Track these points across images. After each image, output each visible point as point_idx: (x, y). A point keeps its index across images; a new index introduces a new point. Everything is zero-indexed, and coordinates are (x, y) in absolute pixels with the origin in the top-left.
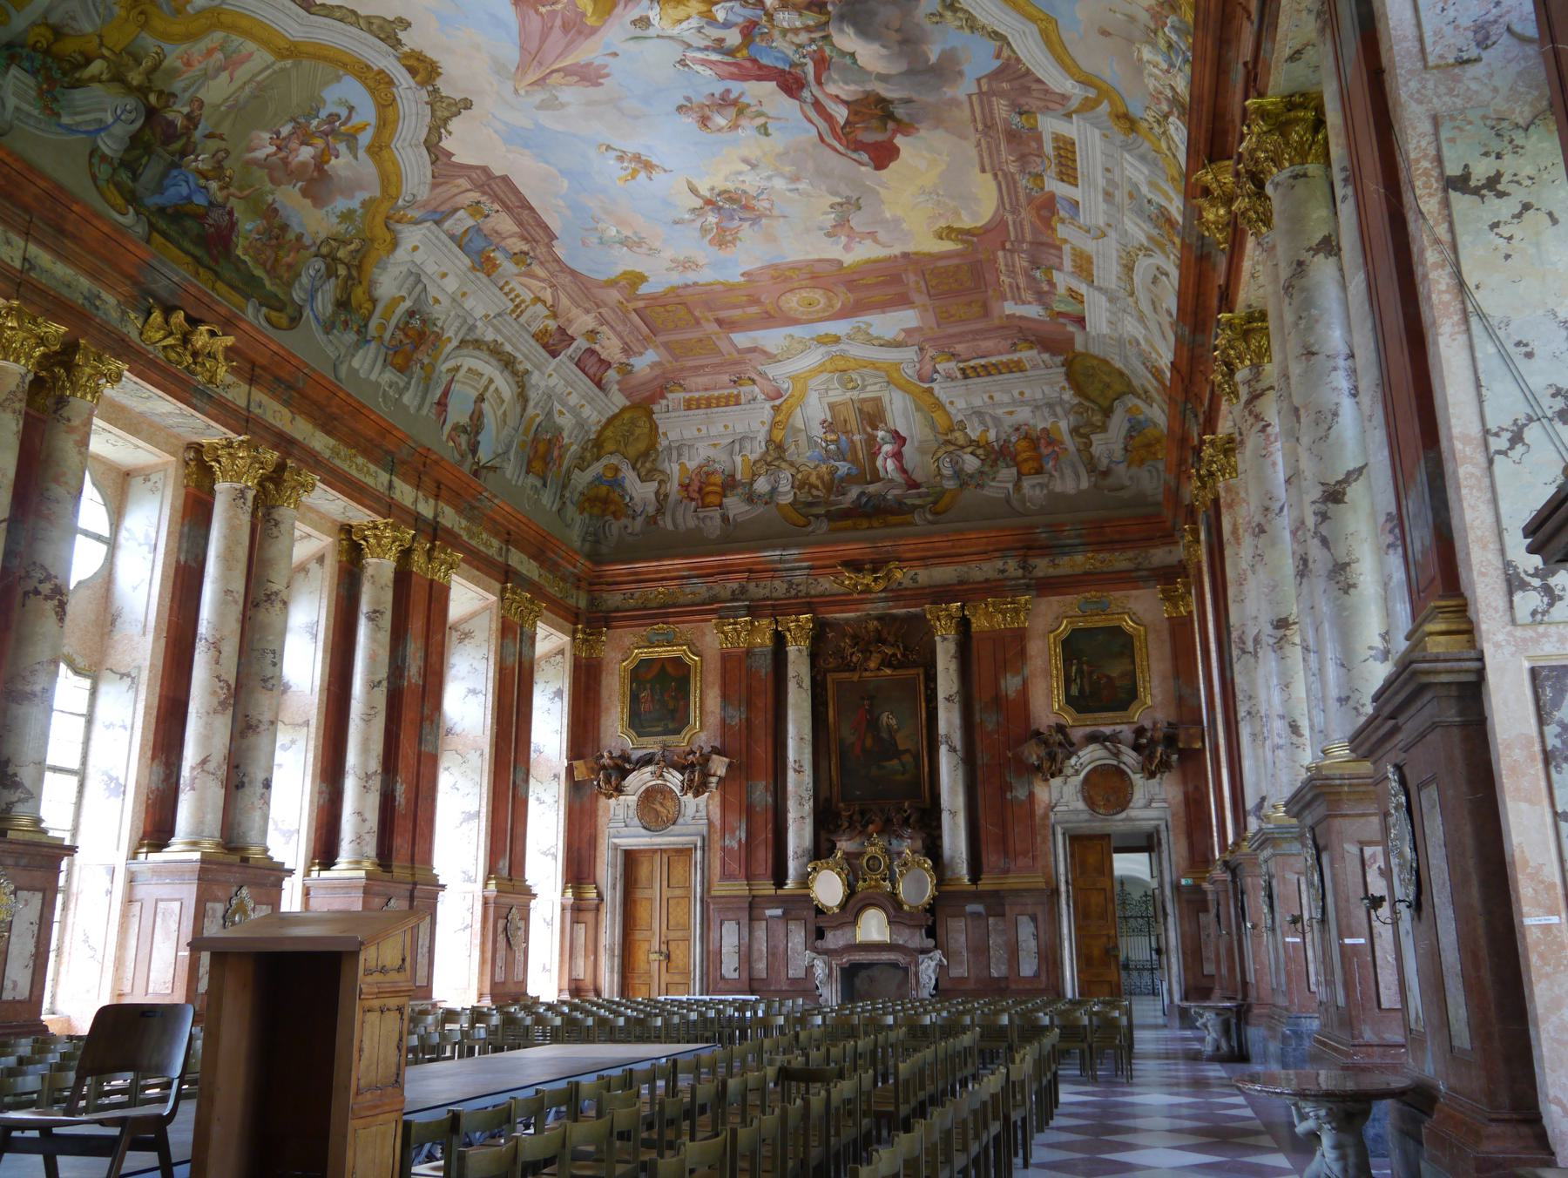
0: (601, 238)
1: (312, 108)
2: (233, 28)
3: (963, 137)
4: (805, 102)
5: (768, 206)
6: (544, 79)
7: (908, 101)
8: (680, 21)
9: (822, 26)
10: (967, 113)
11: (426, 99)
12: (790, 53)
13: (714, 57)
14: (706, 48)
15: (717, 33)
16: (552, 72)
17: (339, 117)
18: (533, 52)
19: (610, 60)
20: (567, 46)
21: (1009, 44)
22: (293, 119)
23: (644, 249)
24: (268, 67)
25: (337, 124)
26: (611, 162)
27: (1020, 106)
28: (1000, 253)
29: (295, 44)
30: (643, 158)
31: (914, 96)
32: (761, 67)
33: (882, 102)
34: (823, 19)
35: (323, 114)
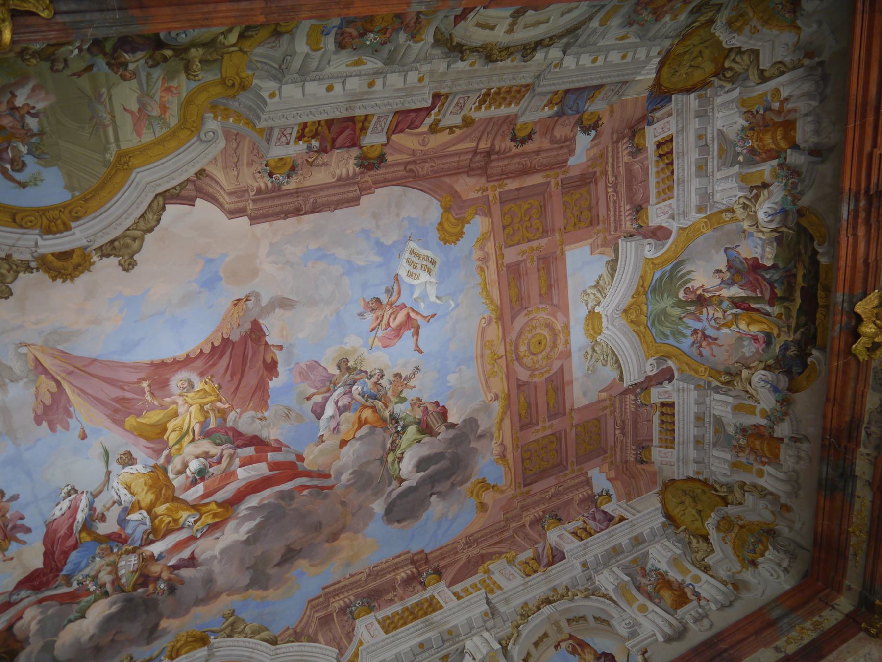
1: (43, 153)
2: (174, 134)
6: (46, 372)
8: (128, 488)
9: (120, 589)
11: (16, 257)
12: (86, 571)
13: (80, 517)
14: (92, 508)
15: (113, 514)
16: (59, 384)
17: (19, 171)
18: (86, 369)
19: (78, 432)
20: (100, 401)
22: (41, 133)
24: (117, 139)
25: (8, 166)
29: (129, 170)
32: (66, 554)
34: (128, 588)
35: (29, 160)
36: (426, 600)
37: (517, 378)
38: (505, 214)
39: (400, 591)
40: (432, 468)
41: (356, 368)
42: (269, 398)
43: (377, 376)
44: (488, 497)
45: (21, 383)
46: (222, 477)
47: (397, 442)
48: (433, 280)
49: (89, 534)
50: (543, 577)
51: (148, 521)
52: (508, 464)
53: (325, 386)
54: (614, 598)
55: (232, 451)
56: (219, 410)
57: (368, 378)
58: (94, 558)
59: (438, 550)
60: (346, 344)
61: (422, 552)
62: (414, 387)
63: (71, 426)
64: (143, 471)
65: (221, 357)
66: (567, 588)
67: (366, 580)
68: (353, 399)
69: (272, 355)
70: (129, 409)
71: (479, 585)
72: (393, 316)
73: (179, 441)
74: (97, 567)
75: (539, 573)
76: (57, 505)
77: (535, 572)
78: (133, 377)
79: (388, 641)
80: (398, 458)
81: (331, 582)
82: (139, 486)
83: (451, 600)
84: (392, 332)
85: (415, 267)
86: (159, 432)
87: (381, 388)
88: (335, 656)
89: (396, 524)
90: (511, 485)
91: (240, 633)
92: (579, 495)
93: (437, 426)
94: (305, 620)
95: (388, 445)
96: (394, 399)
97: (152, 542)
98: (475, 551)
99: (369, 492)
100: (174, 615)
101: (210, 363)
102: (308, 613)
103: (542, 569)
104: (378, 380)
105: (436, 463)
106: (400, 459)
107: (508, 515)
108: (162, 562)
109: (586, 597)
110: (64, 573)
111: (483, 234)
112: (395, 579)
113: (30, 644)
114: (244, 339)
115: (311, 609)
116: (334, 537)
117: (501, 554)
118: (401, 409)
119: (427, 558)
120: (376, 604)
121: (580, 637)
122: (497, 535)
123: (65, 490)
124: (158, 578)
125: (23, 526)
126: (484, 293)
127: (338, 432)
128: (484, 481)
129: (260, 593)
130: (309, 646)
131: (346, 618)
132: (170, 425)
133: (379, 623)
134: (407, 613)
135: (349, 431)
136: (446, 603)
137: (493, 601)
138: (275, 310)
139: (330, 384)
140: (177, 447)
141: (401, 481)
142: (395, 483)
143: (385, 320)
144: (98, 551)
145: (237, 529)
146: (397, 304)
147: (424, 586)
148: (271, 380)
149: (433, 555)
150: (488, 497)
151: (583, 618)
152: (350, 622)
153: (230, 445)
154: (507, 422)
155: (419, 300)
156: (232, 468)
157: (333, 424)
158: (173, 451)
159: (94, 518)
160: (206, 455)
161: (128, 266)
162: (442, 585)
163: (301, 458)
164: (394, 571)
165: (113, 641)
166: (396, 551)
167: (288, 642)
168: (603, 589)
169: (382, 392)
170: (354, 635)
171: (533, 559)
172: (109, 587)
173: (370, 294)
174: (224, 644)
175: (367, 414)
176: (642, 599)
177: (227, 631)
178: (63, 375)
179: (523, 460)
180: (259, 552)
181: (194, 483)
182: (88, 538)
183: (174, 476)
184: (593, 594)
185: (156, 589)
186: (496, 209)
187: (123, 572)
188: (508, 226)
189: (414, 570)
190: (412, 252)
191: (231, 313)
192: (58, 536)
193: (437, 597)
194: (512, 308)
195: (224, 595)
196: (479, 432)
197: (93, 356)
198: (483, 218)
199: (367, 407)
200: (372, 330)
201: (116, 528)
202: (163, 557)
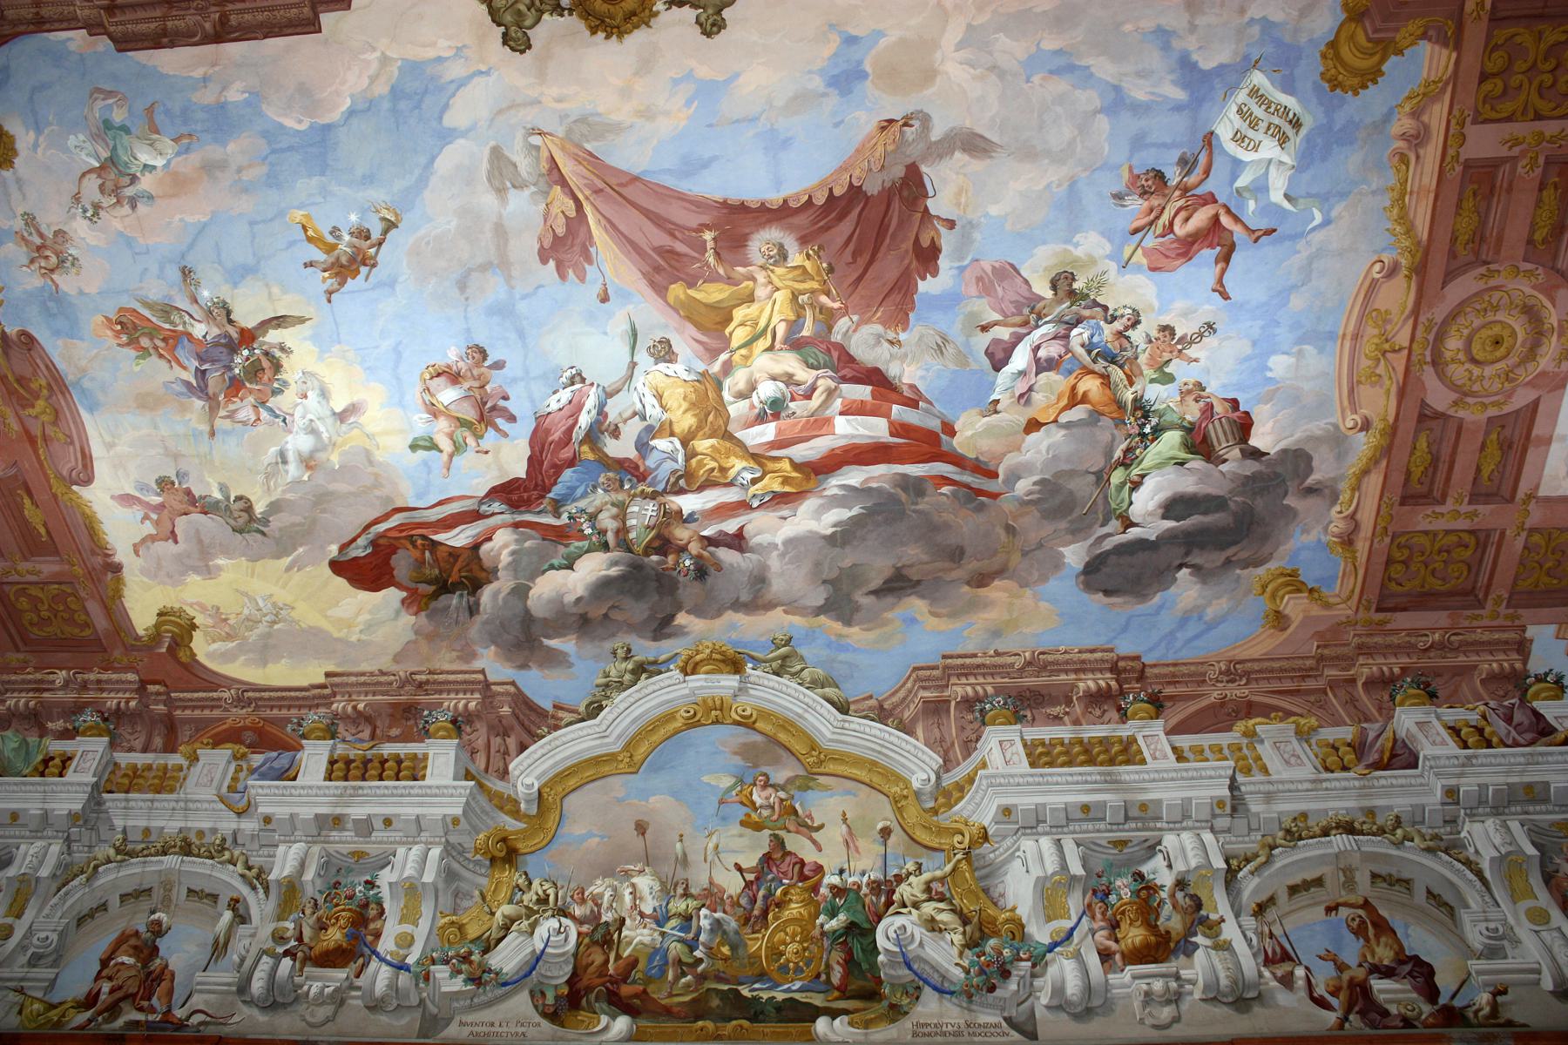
0: (125, 129)
3: (397, 658)
4: (481, 502)
5: (241, 415)
6: (563, 182)
7: (473, 610)
8: (659, 397)
9: (625, 544)
10: (447, 667)
12: (582, 504)
13: (584, 420)
15: (632, 430)
19: (598, 288)
21: (583, 720)
23: (91, 185)
26: (353, 218)
27: (470, 722)
28: (131, 677)
30: (364, 270)
31: (478, 619)
32: (558, 469)
33: (475, 586)
36: (1120, 740)
37: (1423, 401)
38: (1496, 48)
39: (1078, 709)
40: (1194, 520)
41: (1087, 295)
42: (913, 309)
43: (1125, 319)
44: (1295, 606)
45: (527, 192)
46: (808, 422)
47: (1138, 451)
48: (1286, 159)
49: (592, 450)
50: (1357, 783)
51: (680, 457)
52: (1355, 558)
53: (1020, 314)
54: (1487, 874)
55: (833, 384)
56: (822, 309)
57: (1106, 321)
58: (595, 487)
59: (1168, 665)
60: (1077, 245)
61: (1138, 658)
62: (1196, 360)
63: (589, 277)
64: (685, 376)
65: (842, 217)
66: (1398, 822)
67: (1022, 668)
68: (1068, 351)
69: (932, 233)
70: (678, 270)
71: (1226, 752)
72: (1183, 214)
73: (748, 344)
74: (598, 503)
75: (1351, 774)
76: (555, 393)
77: (1345, 768)
78: (693, 220)
79: (1030, 779)
80: (1131, 482)
81: (959, 651)
82: (677, 398)
83: (1165, 757)
84: (1175, 245)
85: (1253, 125)
86: (718, 319)
87: (1128, 345)
88: (935, 768)
89: (1101, 594)
90: (1349, 598)
91: (793, 675)
92: (1490, 664)
93: (1224, 445)
94: (901, 694)
95: (1118, 454)
96: (1149, 373)
97: (681, 491)
98: (1237, 691)
99: (1063, 525)
100: (698, 611)
101: (821, 224)
102: (909, 685)
103: (1360, 769)
104: (1127, 329)
105: (1205, 513)
106: (1136, 485)
107: (1326, 652)
108: (693, 526)
109: (1429, 850)
110: (551, 495)
111: (1427, 84)
112: (1074, 686)
113: (498, 579)
114: (889, 194)
115: (915, 681)
116: (981, 580)
117: (1289, 714)
118: (1158, 394)
119: (1143, 671)
120: (1029, 714)
121: (1383, 912)
122: (1292, 678)
123: (568, 374)
124: (683, 549)
125: (505, 410)
126: (1395, 211)
127: (1028, 402)
128: (1293, 574)
129: (837, 626)
130: (899, 737)
131: (970, 717)
132: (739, 314)
133: (1025, 745)
134: (1077, 749)
135: (1048, 407)
136: (1155, 758)
137: (1243, 788)
138: (953, 154)
139: (1029, 312)
140: (743, 351)
141: (1128, 524)
142: (1115, 524)
143: (1165, 218)
144: (602, 479)
145: (818, 513)
146: (1199, 191)
147: (1124, 716)
148: (923, 278)
149: (1156, 671)
150: (1295, 606)
151: (1406, 883)
152: (976, 725)
153: (830, 373)
154: (1374, 481)
155: (1246, 194)
156: (828, 413)
157: (1021, 387)
158: (736, 357)
159: (604, 428)
160: (789, 379)
161: (712, 27)
162: (1157, 727)
163: (951, 432)
164: (1076, 671)
165: (606, 616)
166: (1090, 643)
167: (865, 717)
168: (1472, 850)
169: (1129, 354)
170: (976, 749)
171: (1349, 745)
172: (610, 537)
173: (1148, 159)
174: (766, 683)
175: (1090, 385)
176: (1544, 898)
177: (775, 665)
178: (588, 192)
179: (1389, 562)
180: (847, 563)
181: (761, 419)
182: (591, 456)
183: (732, 399)
184: (1446, 852)
185: (677, 563)
186: (1475, 33)
187: (634, 522)
188: (1494, 75)
189: (1113, 683)
190: (1255, 93)
191: (874, 141)
192: (550, 439)
193: (1141, 741)
194: (1452, 254)
195: (780, 609)
196: (1310, 481)
197: (636, 171)
198: (1437, 48)
199: (1092, 372)
200: (1135, 231)
201: (631, 453)
202: (696, 520)
